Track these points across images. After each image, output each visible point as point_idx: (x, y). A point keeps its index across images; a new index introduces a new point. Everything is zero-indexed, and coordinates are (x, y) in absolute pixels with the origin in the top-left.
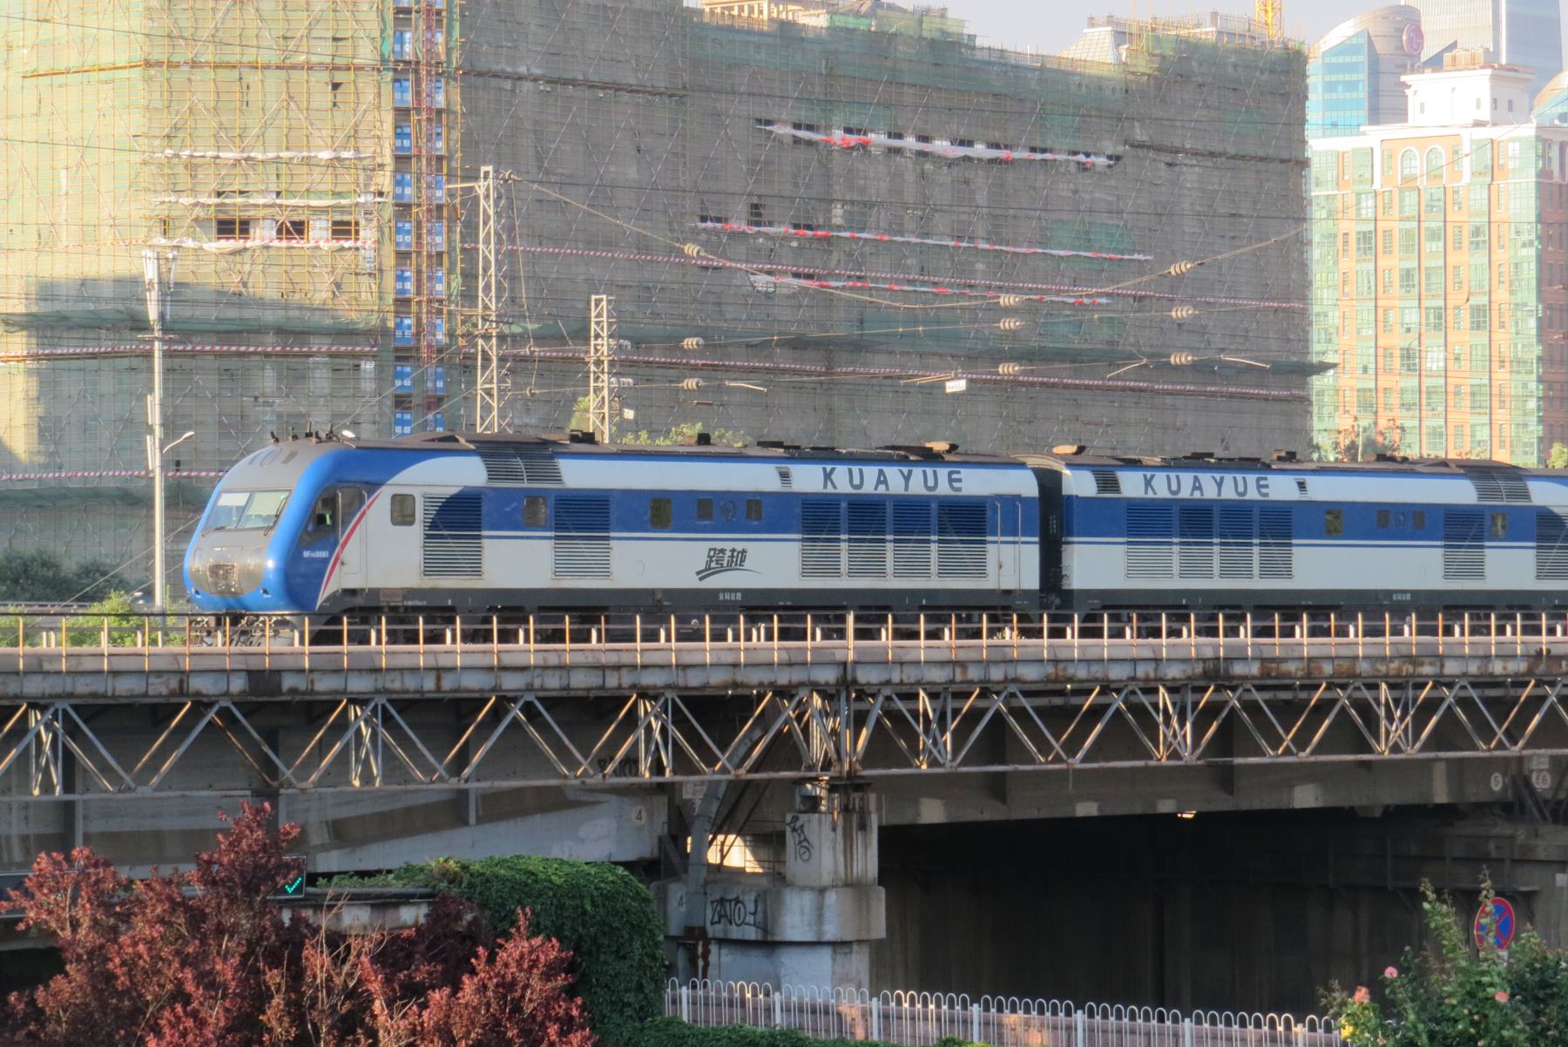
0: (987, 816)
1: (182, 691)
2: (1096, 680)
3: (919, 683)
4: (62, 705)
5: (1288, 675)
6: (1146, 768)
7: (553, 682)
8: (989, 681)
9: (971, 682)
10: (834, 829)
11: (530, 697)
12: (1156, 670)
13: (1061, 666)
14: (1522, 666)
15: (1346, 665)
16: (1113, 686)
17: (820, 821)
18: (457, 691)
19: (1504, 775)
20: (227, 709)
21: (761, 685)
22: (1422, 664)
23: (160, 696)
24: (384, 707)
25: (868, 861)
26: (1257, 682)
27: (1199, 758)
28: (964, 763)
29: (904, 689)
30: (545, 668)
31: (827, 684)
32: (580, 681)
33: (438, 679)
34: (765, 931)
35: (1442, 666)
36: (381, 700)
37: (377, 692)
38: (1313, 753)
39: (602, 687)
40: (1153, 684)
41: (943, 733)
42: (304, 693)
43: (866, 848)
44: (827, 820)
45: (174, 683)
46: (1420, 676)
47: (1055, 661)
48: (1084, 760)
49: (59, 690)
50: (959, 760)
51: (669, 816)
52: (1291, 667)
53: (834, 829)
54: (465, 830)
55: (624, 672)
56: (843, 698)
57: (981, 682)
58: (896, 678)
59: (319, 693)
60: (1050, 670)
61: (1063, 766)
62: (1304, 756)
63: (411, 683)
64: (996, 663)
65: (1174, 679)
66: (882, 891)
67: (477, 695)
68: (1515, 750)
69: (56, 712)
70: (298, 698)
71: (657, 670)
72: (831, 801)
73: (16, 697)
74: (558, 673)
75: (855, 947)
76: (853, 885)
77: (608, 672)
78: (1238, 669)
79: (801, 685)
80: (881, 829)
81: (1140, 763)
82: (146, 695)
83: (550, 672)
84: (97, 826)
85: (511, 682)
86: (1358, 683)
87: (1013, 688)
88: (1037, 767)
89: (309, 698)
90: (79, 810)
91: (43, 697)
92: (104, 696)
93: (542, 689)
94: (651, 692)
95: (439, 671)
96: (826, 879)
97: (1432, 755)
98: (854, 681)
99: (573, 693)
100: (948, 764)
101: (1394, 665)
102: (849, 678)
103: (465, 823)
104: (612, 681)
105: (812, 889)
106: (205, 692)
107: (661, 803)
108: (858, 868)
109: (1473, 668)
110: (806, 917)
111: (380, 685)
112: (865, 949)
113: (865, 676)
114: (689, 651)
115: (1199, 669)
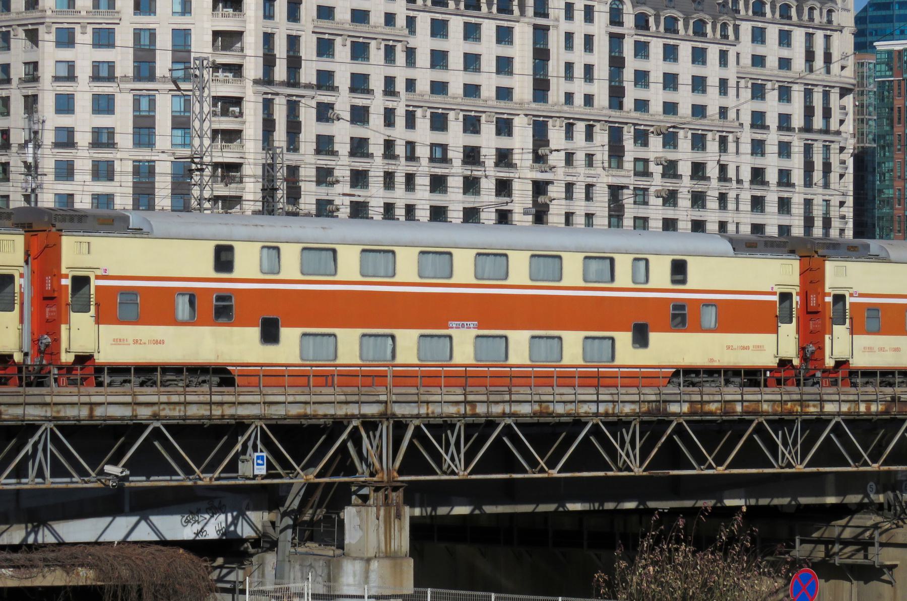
2: (569, 415)
5: (711, 413)
6: (607, 477)
9: (477, 416)
11: (157, 424)
12: (614, 408)
13: (544, 405)
14: (881, 408)
15: (753, 406)
16: (583, 419)
17: (367, 512)
19: (877, 484)
21: (325, 416)
22: (808, 406)
24: (51, 430)
25: (402, 540)
26: (688, 418)
27: (644, 471)
28: (470, 474)
29: (432, 421)
31: (373, 416)
32: (193, 411)
33: (91, 410)
34: (329, 587)
35: (822, 407)
36: (51, 425)
38: (727, 468)
39: (210, 418)
40: (611, 419)
41: (459, 452)
43: (400, 530)
46: (807, 414)
47: (541, 402)
48: (559, 472)
50: (469, 471)
52: (713, 407)
55: (226, 406)
58: (423, 410)
60: (536, 407)
61: (545, 475)
62: (721, 470)
63: (71, 412)
64: (497, 402)
65: (627, 415)
68: (875, 467)
71: (250, 406)
74: (178, 408)
76: (390, 556)
77: (214, 407)
78: (674, 408)
79: (353, 417)
80: (412, 519)
81: (601, 474)
83: (172, 407)
85: (144, 412)
86: (762, 419)
87: (509, 421)
88: (526, 476)
93: (166, 418)
95: (91, 404)
96: (371, 554)
97: (814, 469)
98: (394, 415)
99: (188, 422)
100: (461, 473)
101: (789, 404)
102: (389, 412)
104: (217, 412)
105: (362, 559)
108: (395, 545)
109: (845, 408)
110: (357, 578)
111: (49, 414)
113: (399, 410)
115: (645, 407)
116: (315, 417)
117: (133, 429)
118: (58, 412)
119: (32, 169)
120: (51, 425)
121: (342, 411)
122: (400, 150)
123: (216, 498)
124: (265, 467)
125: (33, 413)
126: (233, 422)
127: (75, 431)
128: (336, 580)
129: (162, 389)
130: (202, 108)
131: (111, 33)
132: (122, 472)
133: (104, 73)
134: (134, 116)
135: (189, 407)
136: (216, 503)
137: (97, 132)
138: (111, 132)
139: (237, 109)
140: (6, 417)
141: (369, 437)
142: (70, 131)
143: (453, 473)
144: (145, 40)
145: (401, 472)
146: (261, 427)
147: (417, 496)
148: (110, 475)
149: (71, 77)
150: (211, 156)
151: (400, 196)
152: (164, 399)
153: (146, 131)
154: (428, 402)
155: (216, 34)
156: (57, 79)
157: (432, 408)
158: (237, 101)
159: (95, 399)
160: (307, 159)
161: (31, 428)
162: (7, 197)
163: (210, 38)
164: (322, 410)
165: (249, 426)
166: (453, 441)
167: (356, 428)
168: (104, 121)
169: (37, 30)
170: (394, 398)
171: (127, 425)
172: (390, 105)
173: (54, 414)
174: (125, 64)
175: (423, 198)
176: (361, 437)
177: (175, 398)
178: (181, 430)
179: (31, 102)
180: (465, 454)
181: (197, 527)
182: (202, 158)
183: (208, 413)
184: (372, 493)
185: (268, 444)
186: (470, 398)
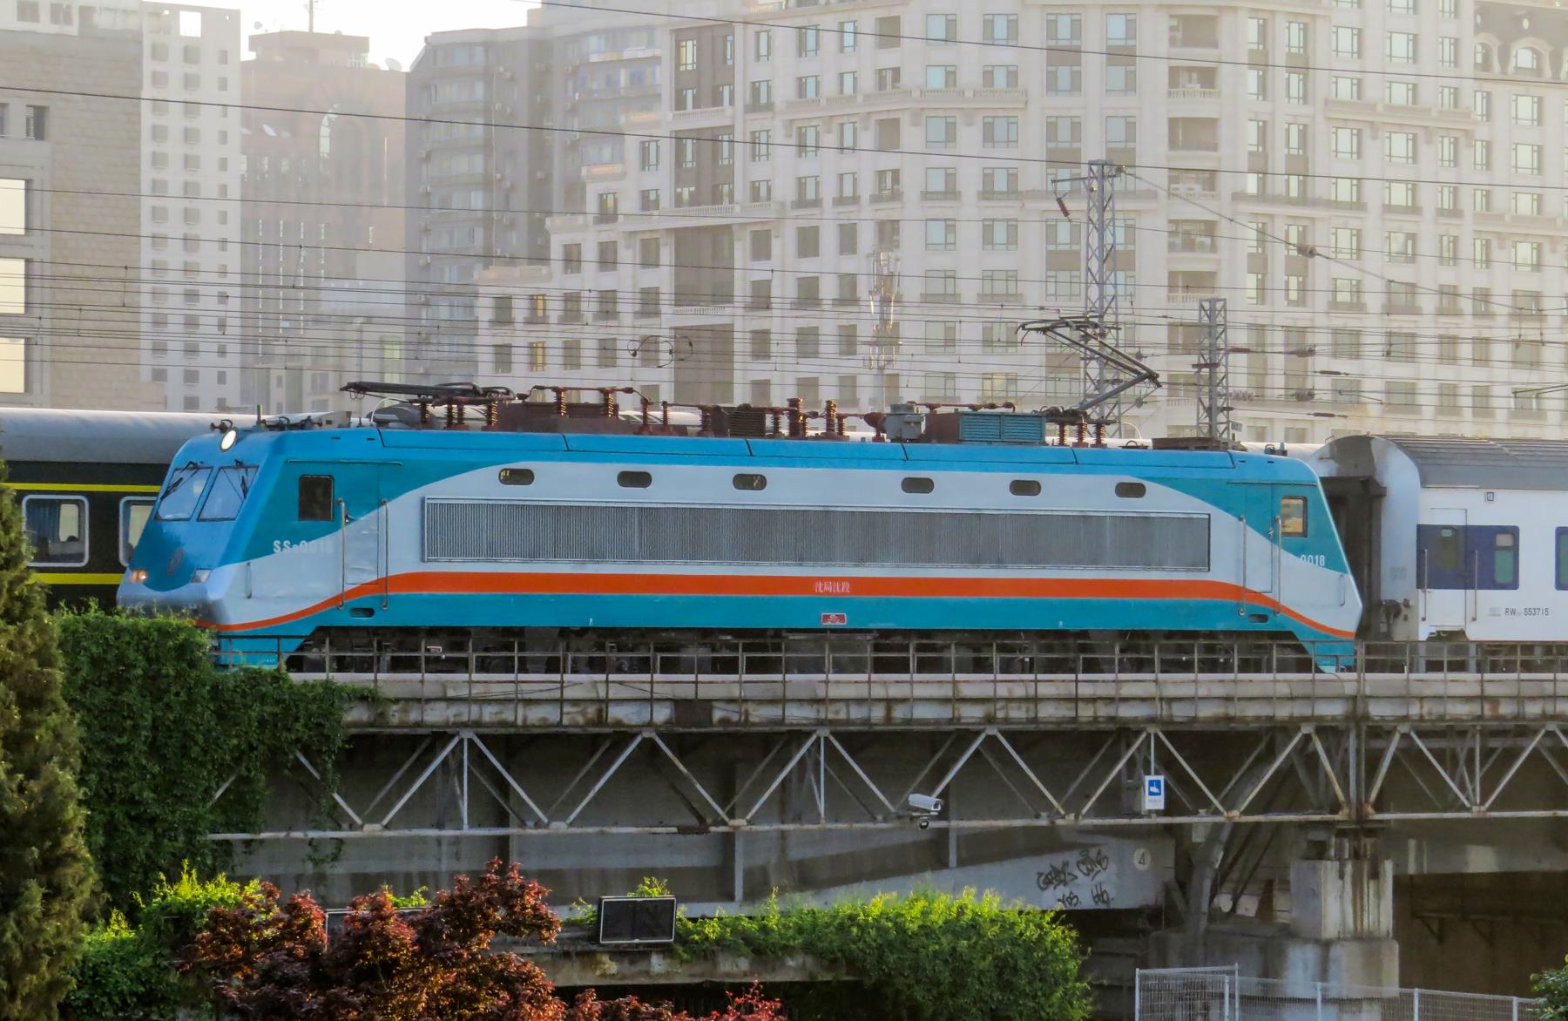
0: (1545, 866)
1: (600, 719)
3: (1441, 718)
4: (467, 734)
7: (1018, 713)
8: (1524, 718)
9: (1502, 718)
10: (1342, 876)
11: (992, 731)
18: (908, 721)
20: (651, 740)
21: (1258, 718)
23: (576, 726)
24: (826, 739)
25: (1381, 913)
28: (1490, 809)
29: (1427, 726)
30: (1009, 700)
31: (1334, 718)
32: (1047, 712)
33: (889, 710)
36: (824, 732)
37: (821, 723)
39: (1074, 720)
42: (737, 724)
43: (1378, 896)
44: (1329, 868)
45: (591, 711)
49: (465, 718)
50: (1487, 805)
51: (1177, 863)
53: (1342, 876)
54: (945, 872)
55: (1100, 704)
56: (1352, 736)
57: (1516, 717)
58: (1414, 710)
59: (753, 724)
63: (857, 713)
64: (1533, 699)
66: (1396, 946)
67: (931, 728)
69: (461, 741)
70: (731, 729)
71: (1137, 703)
72: (1340, 849)
73: (418, 724)
74: (1024, 706)
75: (1365, 1006)
77: (1080, 705)
79: (1306, 719)
80: (1396, 879)
82: (560, 724)
83: (1014, 705)
84: (534, 864)
85: (971, 713)
89: (743, 729)
90: (514, 846)
91: (447, 725)
92: (513, 725)
93: (1007, 720)
94: (1133, 727)
95: (890, 702)
98: (1367, 717)
99: (1042, 727)
100: (1475, 809)
103: (941, 863)
104: (1086, 712)
105: (1317, 941)
106: (626, 721)
107: (1169, 846)
108: (1368, 921)
111: (822, 716)
112: (1377, 1008)
113: (1377, 710)
114: (1174, 683)
116: (1243, 720)
117: (953, 738)
118: (837, 712)
119: (887, 338)
120: (824, 732)
121: (1283, 712)
122: (1466, 305)
123: (1094, 845)
124: (1162, 798)
125: (797, 714)
126: (1111, 726)
127: (860, 740)
128: (1277, 975)
129: (1000, 677)
130: (1101, 238)
131: (1011, 122)
132: (936, 806)
133: (1001, 184)
134: (1050, 254)
135: (1040, 706)
136: (1093, 853)
137: (988, 277)
138: (1012, 277)
139: (1208, 240)
140: (756, 720)
141: (1328, 752)
142: (950, 276)
143: (1463, 808)
144: (1064, 133)
145: (1379, 806)
146: (1156, 736)
147: (1412, 843)
148: (917, 809)
149: (951, 193)
150: (1116, 314)
151: (1467, 375)
152: (1002, 691)
153: (1064, 276)
154: (1422, 699)
155: (1173, 123)
156: (927, 195)
157: (1427, 707)
158: (1210, 228)
159: (894, 692)
160: (1320, 322)
161: (797, 736)
162: (853, 378)
163: (1164, 130)
164: (1252, 711)
165: (1138, 733)
166: (1462, 756)
167: (1307, 738)
168: (1001, 260)
169: (897, 121)
170: (1368, 692)
171: (948, 733)
172: (1453, 232)
173: (831, 716)
174: (1034, 176)
175: (1503, 376)
176: (1315, 753)
177: (1019, 691)
178: (1031, 740)
179: (888, 232)
180: (1483, 780)
181: (1062, 891)
182: (1101, 317)
183: (1073, 714)
184: (1333, 840)
185: (1167, 764)
186: (1491, 690)
